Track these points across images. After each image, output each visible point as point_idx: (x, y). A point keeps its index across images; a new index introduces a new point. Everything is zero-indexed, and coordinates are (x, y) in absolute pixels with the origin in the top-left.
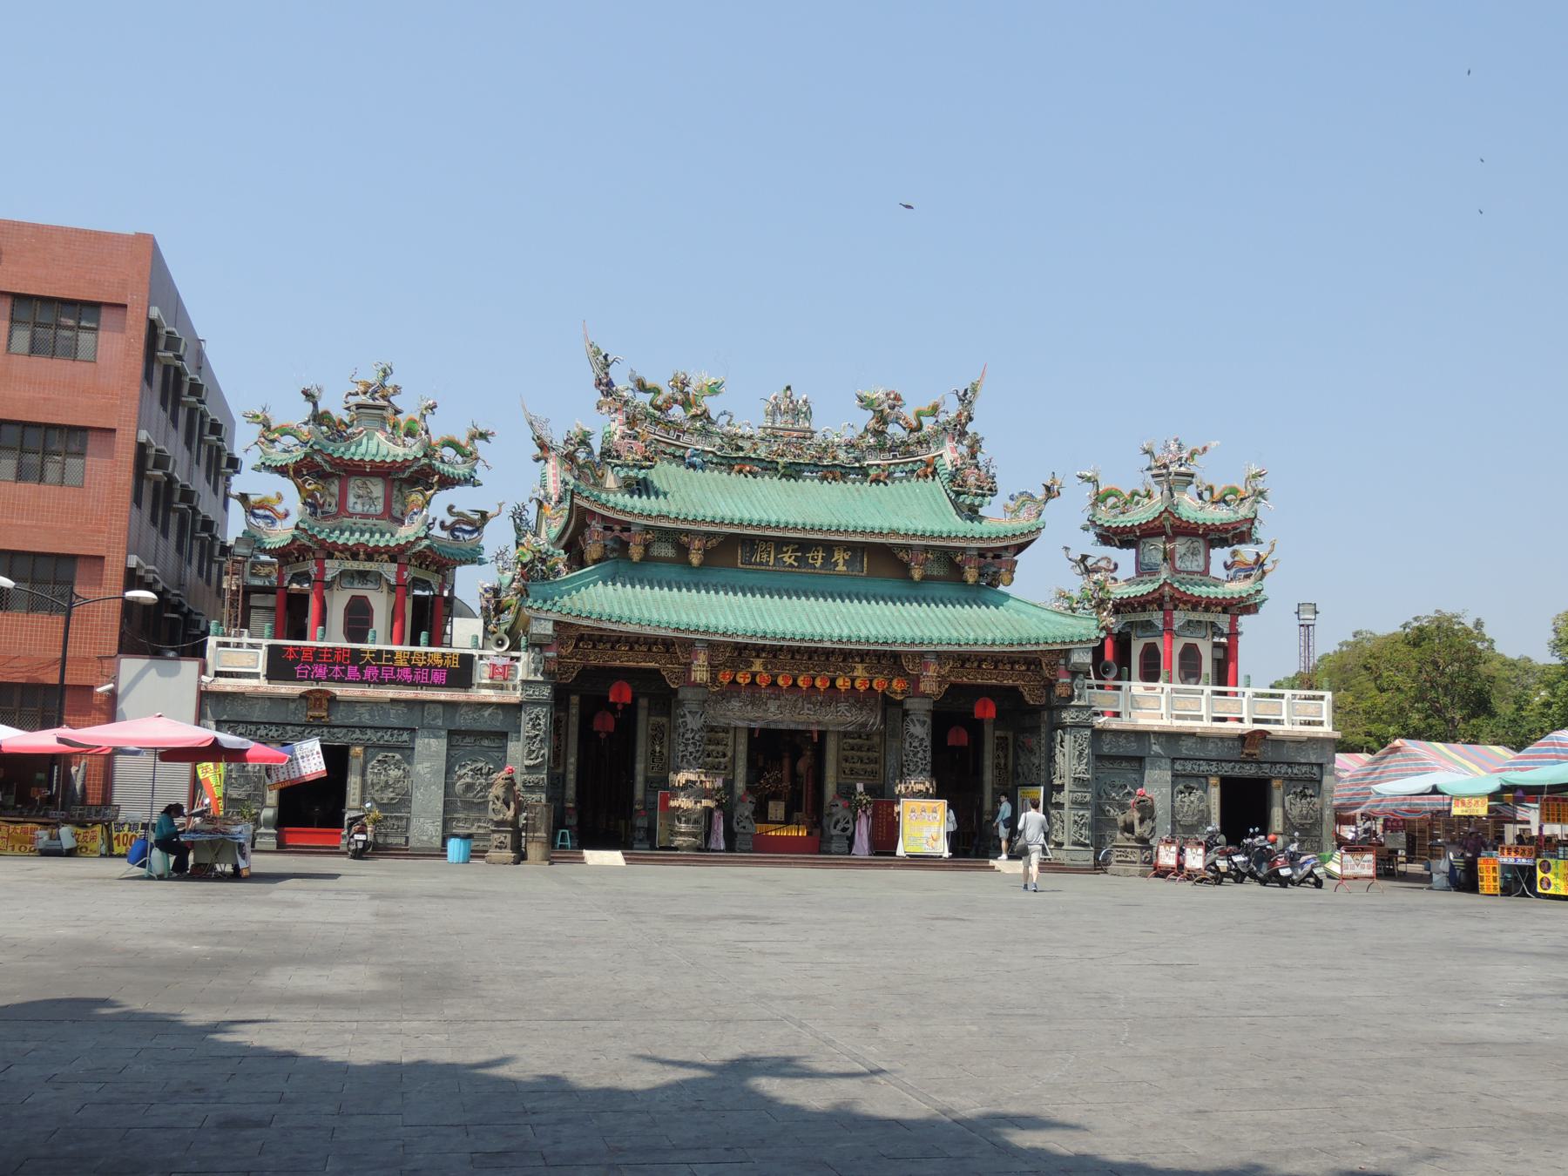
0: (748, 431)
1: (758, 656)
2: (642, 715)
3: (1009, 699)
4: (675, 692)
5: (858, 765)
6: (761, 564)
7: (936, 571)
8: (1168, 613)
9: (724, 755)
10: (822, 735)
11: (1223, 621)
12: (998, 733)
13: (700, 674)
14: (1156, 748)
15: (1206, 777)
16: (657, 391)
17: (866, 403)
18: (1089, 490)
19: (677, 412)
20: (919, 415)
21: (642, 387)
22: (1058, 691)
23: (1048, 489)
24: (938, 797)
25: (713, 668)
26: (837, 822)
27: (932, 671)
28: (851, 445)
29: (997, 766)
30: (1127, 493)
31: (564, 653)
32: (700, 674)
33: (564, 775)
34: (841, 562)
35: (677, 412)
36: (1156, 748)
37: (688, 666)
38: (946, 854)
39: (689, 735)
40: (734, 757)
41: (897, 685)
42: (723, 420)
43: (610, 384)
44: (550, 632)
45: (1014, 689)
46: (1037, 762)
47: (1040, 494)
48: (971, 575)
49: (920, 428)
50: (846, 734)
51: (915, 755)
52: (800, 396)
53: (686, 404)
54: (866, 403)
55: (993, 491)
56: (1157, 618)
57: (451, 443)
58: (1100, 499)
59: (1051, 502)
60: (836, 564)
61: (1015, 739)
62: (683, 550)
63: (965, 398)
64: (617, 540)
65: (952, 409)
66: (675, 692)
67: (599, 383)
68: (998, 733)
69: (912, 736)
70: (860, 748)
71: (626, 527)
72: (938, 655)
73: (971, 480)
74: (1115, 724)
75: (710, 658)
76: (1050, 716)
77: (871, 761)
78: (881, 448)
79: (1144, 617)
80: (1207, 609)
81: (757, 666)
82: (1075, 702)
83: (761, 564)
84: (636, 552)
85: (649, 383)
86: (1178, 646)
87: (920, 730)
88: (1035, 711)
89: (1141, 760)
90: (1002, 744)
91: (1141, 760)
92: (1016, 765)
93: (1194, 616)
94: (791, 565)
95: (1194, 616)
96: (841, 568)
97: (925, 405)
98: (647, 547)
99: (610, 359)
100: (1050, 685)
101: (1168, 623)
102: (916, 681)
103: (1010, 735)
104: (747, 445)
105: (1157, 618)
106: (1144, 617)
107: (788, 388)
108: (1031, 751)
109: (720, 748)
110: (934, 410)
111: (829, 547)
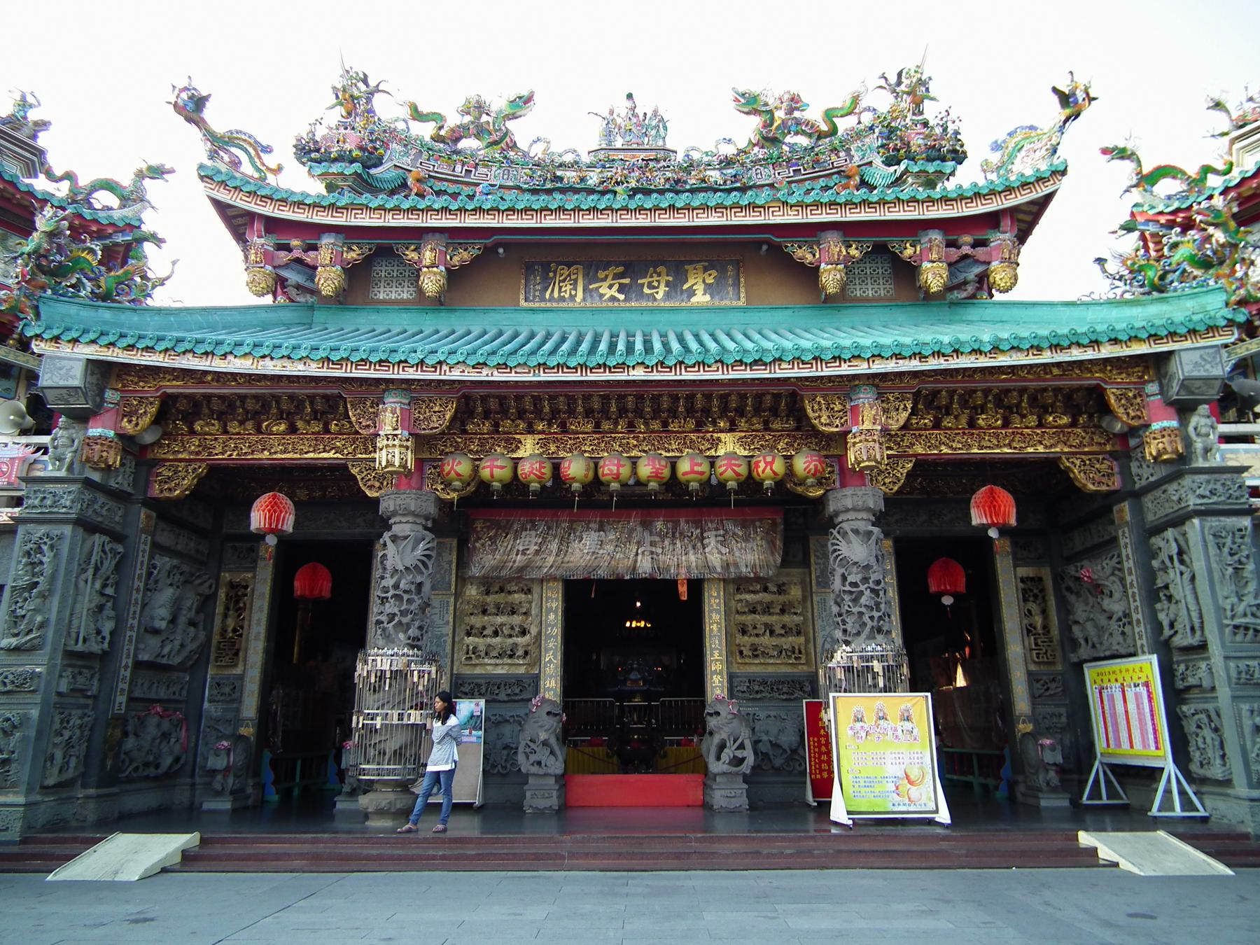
0: (568, 158)
1: (530, 430)
3: (1040, 484)
4: (376, 501)
5: (766, 640)
6: (562, 299)
9: (524, 632)
10: (696, 586)
12: (1023, 571)
16: (436, 117)
17: (750, 103)
18: (1126, 169)
20: (829, 115)
21: (417, 115)
22: (1152, 449)
23: (1065, 99)
24: (915, 687)
25: (427, 446)
26: (722, 747)
28: (727, 162)
29: (1029, 630)
30: (1192, 171)
31: (127, 427)
33: (241, 678)
34: (700, 288)
38: (944, 816)
39: (389, 582)
40: (540, 633)
41: (804, 463)
44: (76, 382)
45: (1050, 465)
46: (1117, 608)
48: (934, 275)
49: (833, 131)
50: (737, 584)
51: (856, 601)
53: (480, 132)
54: (750, 103)
55: (959, 156)
57: (109, 186)
59: (1073, 126)
60: (691, 293)
61: (1058, 578)
66: (376, 501)
68: (1023, 571)
69: (845, 562)
70: (767, 609)
72: (878, 381)
76: (1139, 511)
77: (787, 631)
82: (1200, 463)
83: (562, 299)
85: (424, 108)
87: (858, 549)
88: (1103, 505)
90: (1031, 590)
92: (1066, 627)
94: (613, 299)
96: (701, 298)
97: (839, 100)
99: (372, 83)
100: (1126, 445)
103: (1046, 573)
107: (630, 96)
108: (1097, 589)
109: (516, 620)
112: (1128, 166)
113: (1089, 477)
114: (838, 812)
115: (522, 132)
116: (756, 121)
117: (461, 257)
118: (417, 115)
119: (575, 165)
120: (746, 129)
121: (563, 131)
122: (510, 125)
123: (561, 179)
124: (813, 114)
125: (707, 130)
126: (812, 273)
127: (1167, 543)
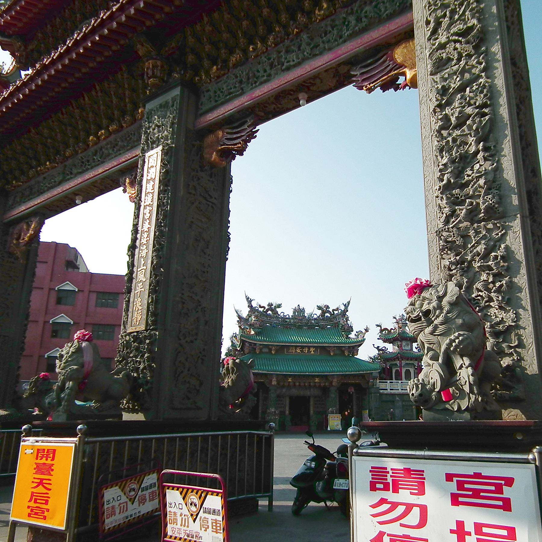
0: (287, 316)
2: (261, 394)
7: (338, 352)
8: (401, 362)
10: (309, 397)
11: (416, 363)
13: (274, 383)
14: (397, 398)
15: (412, 406)
16: (264, 307)
17: (319, 308)
19: (270, 312)
21: (260, 307)
27: (335, 380)
32: (274, 383)
35: (270, 312)
36: (397, 398)
37: (271, 382)
42: (282, 314)
43: (252, 306)
47: (364, 331)
50: (315, 397)
52: (301, 307)
54: (319, 308)
56: (398, 362)
58: (381, 331)
62: (270, 350)
63: (346, 306)
64: (253, 348)
65: (343, 308)
67: (249, 306)
71: (255, 344)
73: (346, 327)
74: (385, 392)
75: (277, 379)
78: (323, 319)
79: (395, 362)
80: (411, 360)
81: (290, 380)
84: (258, 351)
85: (262, 306)
86: (404, 371)
89: (393, 401)
91: (393, 401)
93: (407, 362)
95: (407, 362)
98: (261, 349)
100: (368, 382)
101: (401, 364)
102: (331, 383)
104: (288, 320)
105: (398, 362)
106: (395, 362)
110: (337, 309)
111: (309, 347)
112: (379, 328)
113: (364, 386)
114: (329, 429)
115: (279, 310)
116: (320, 311)
117: (278, 347)
118: (260, 307)
119: (289, 318)
120: (319, 312)
121: (287, 311)
122: (277, 309)
123: (286, 322)
124: (331, 310)
125: (312, 310)
126: (329, 352)
127: (370, 396)
